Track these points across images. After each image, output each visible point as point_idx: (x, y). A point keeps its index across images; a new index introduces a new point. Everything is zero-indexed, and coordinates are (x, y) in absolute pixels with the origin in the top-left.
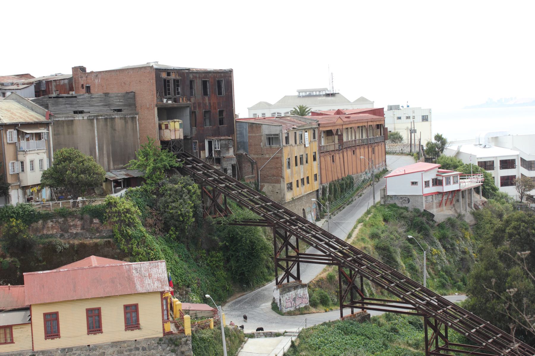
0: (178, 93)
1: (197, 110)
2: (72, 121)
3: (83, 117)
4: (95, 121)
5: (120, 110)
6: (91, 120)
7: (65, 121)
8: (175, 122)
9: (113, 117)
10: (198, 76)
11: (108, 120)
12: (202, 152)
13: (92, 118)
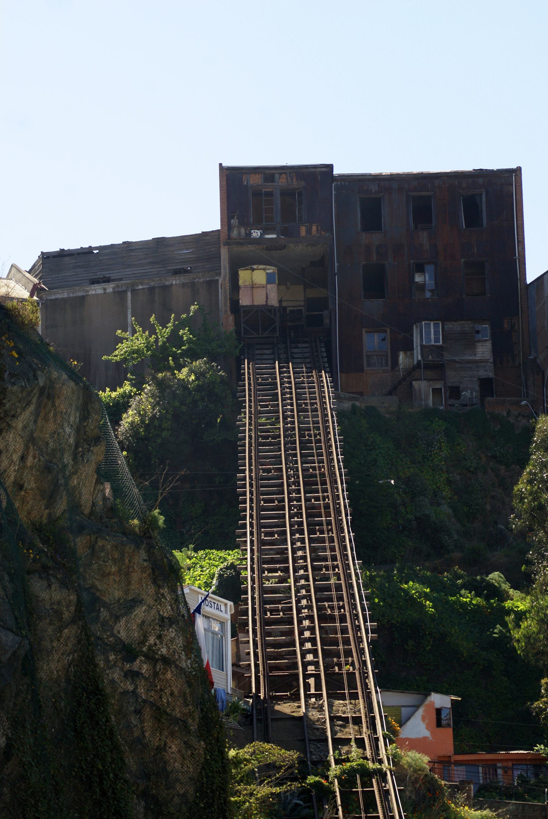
2: (83, 298)
3: (105, 289)
4: (129, 294)
5: (186, 271)
6: (120, 294)
7: (69, 298)
8: (253, 270)
9: (167, 283)
11: (157, 290)
12: (401, 356)
13: (124, 289)
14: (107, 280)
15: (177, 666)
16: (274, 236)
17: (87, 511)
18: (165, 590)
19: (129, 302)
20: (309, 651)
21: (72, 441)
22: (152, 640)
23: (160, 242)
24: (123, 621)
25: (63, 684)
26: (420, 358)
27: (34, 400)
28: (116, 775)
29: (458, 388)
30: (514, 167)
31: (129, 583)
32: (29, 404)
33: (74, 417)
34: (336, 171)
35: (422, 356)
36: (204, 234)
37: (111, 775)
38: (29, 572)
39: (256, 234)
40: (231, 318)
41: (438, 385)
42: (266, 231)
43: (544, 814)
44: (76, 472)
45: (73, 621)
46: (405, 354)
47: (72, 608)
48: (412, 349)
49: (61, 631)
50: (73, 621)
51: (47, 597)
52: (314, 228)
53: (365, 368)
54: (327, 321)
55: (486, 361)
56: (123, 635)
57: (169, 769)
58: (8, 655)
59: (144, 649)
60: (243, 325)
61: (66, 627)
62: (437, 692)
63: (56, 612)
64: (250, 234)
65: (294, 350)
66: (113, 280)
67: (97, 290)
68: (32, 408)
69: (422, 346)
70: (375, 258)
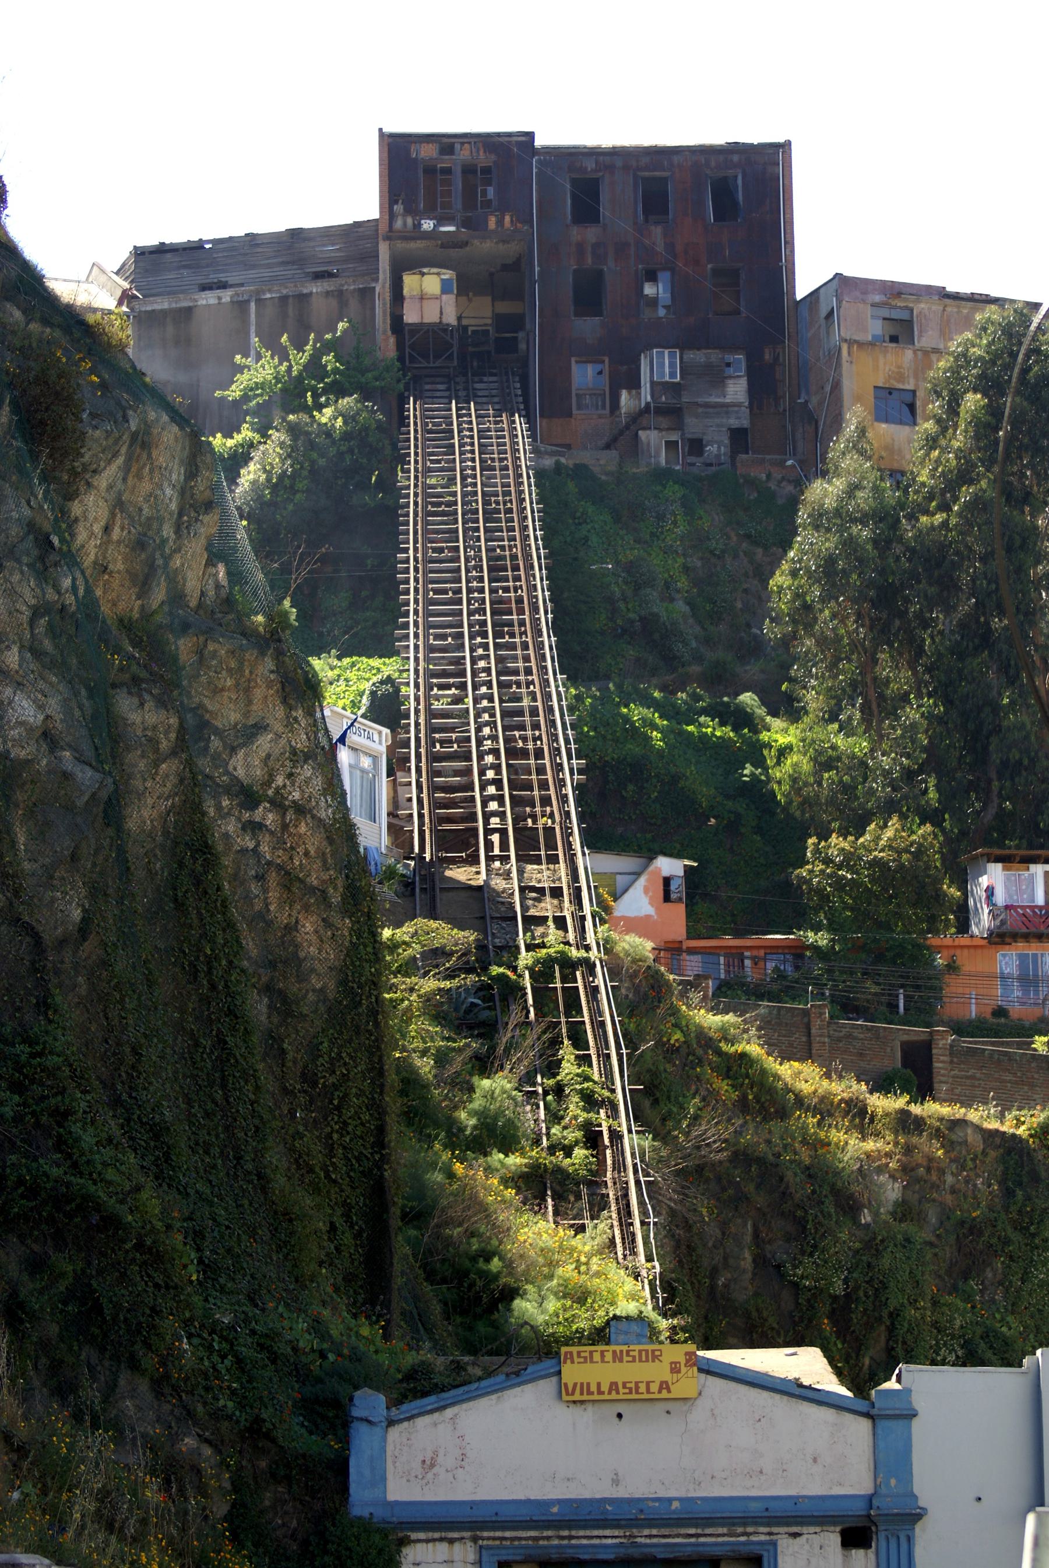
0: (487, 204)
1: (611, 263)
2: (189, 310)
3: (220, 298)
4: (253, 305)
5: (330, 275)
6: (240, 306)
7: (171, 310)
8: (423, 274)
9: (305, 291)
10: (619, 163)
11: (291, 300)
12: (624, 395)
13: (246, 297)
14: (223, 286)
15: (313, 817)
16: (452, 229)
17: (193, 603)
18: (299, 713)
19: (253, 316)
20: (492, 798)
21: (174, 506)
22: (280, 780)
23: (295, 234)
24: (241, 753)
25: (159, 839)
26: (649, 398)
27: (124, 450)
28: (231, 962)
29: (700, 441)
30: (782, 140)
31: (250, 702)
32: (115, 455)
33: (177, 475)
34: (539, 142)
35: (652, 396)
36: (357, 224)
37: (224, 962)
38: (114, 686)
39: (428, 225)
40: (392, 340)
41: (674, 437)
42: (441, 221)
43: (806, 1020)
44: (178, 550)
45: (174, 753)
46: (630, 393)
47: (173, 736)
48: (639, 387)
49: (157, 766)
50: (174, 753)
51: (138, 720)
52: (507, 219)
53: (575, 412)
54: (522, 346)
55: (739, 405)
56: (240, 773)
57: (302, 955)
58: (86, 798)
59: (270, 792)
60: (407, 350)
61: (164, 761)
62: (665, 854)
63: (150, 740)
64: (420, 225)
65: (478, 386)
66: (231, 286)
67: (208, 299)
68: (120, 460)
69: (652, 382)
70: (590, 261)
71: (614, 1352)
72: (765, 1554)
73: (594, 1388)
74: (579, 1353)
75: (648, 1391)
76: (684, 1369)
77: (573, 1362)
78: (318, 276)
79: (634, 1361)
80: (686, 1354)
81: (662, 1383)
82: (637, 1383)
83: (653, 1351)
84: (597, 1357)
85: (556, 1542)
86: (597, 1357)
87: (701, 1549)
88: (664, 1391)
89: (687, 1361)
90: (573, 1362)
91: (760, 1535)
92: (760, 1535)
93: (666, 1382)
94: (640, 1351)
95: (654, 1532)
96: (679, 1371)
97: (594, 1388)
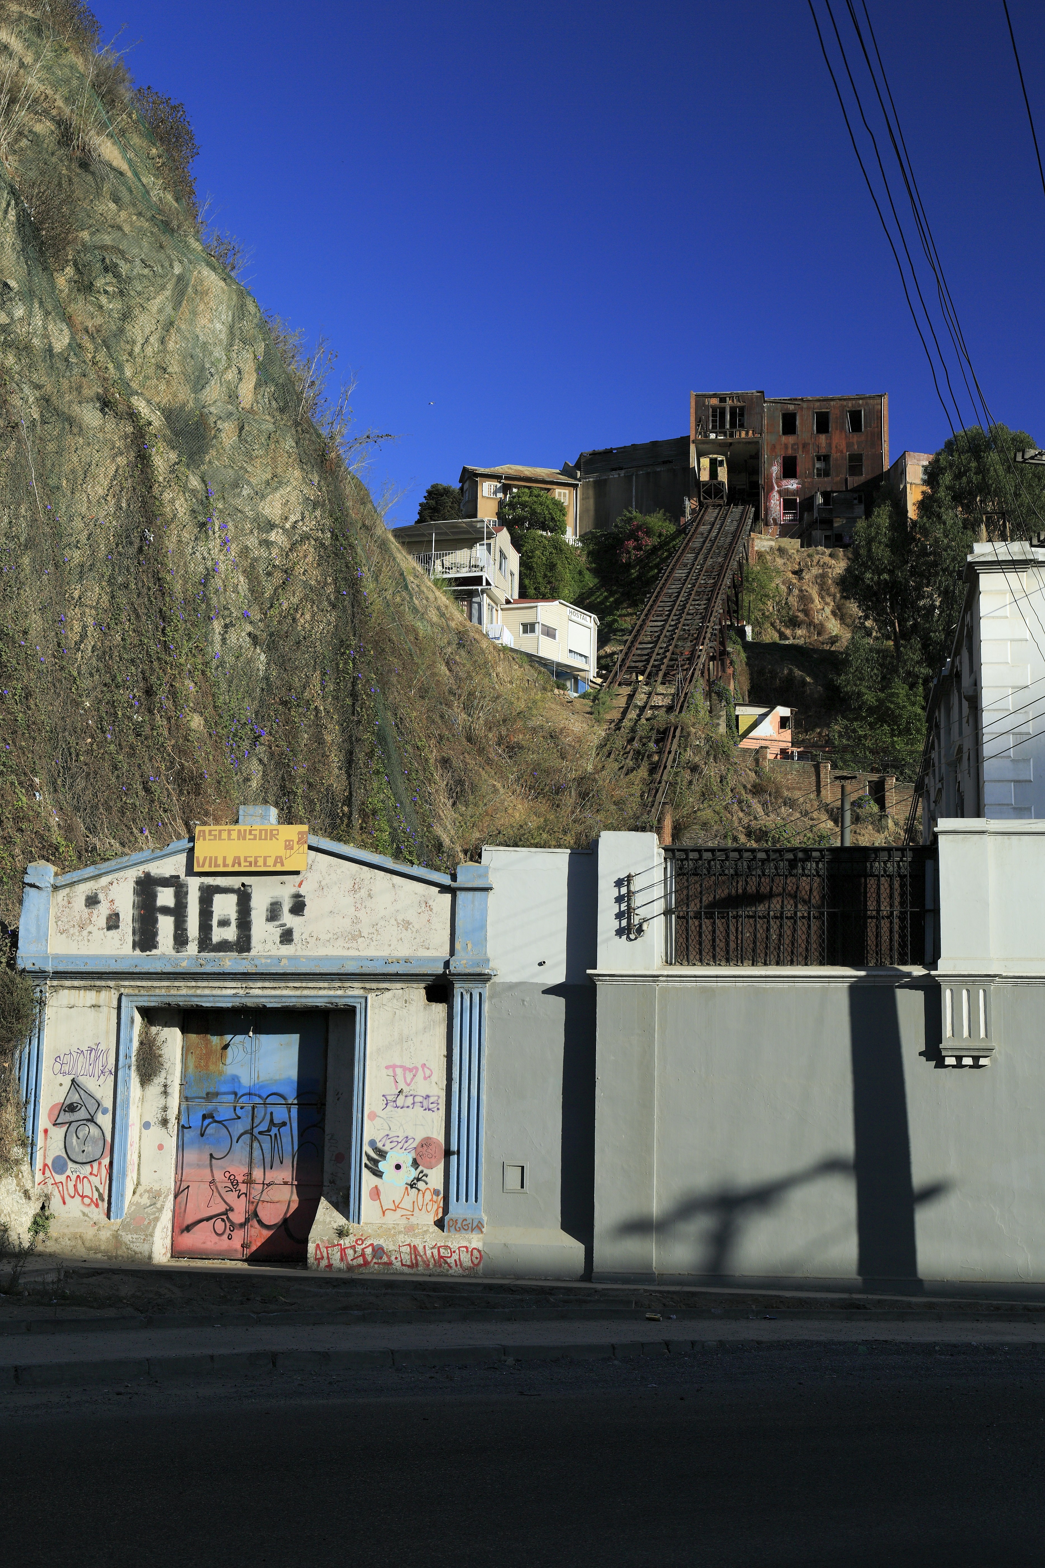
1: (800, 452)
2: (605, 480)
5: (670, 462)
6: (629, 478)
12: (806, 515)
14: (621, 469)
23: (654, 443)
32: (163, 288)
39: (713, 436)
52: (751, 432)
67: (614, 475)
71: (239, 831)
72: (358, 1006)
73: (220, 861)
74: (210, 831)
75: (265, 864)
76: (296, 846)
77: (204, 839)
78: (664, 463)
79: (255, 839)
80: (299, 833)
81: (277, 858)
82: (256, 858)
83: (271, 831)
84: (225, 835)
85: (184, 992)
86: (225, 835)
87: (303, 1000)
88: (279, 865)
89: (300, 839)
90: (204, 839)
91: (353, 992)
92: (353, 992)
93: (281, 857)
94: (261, 831)
95: (267, 984)
96: (292, 848)
97: (220, 861)
